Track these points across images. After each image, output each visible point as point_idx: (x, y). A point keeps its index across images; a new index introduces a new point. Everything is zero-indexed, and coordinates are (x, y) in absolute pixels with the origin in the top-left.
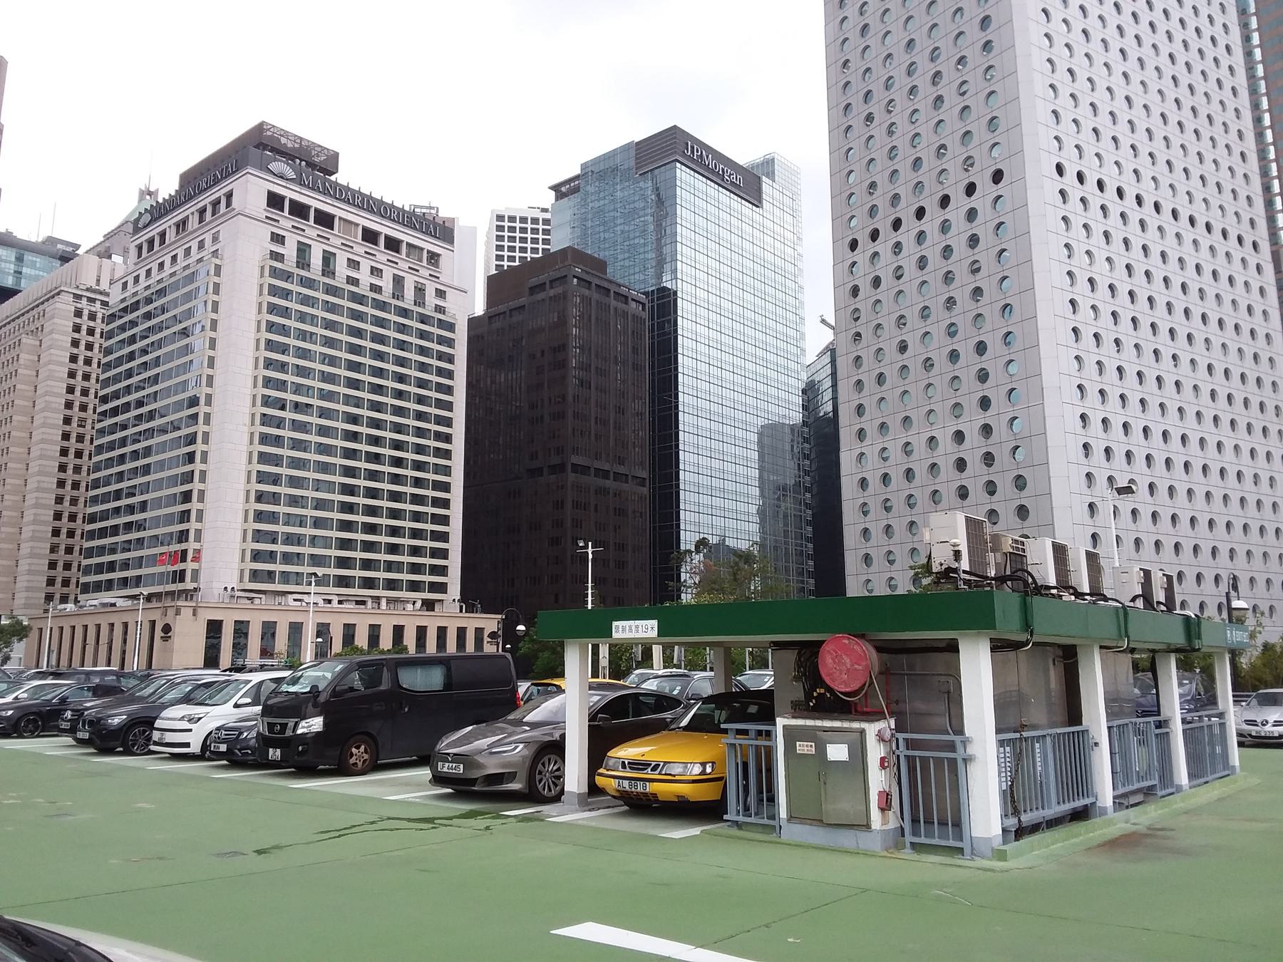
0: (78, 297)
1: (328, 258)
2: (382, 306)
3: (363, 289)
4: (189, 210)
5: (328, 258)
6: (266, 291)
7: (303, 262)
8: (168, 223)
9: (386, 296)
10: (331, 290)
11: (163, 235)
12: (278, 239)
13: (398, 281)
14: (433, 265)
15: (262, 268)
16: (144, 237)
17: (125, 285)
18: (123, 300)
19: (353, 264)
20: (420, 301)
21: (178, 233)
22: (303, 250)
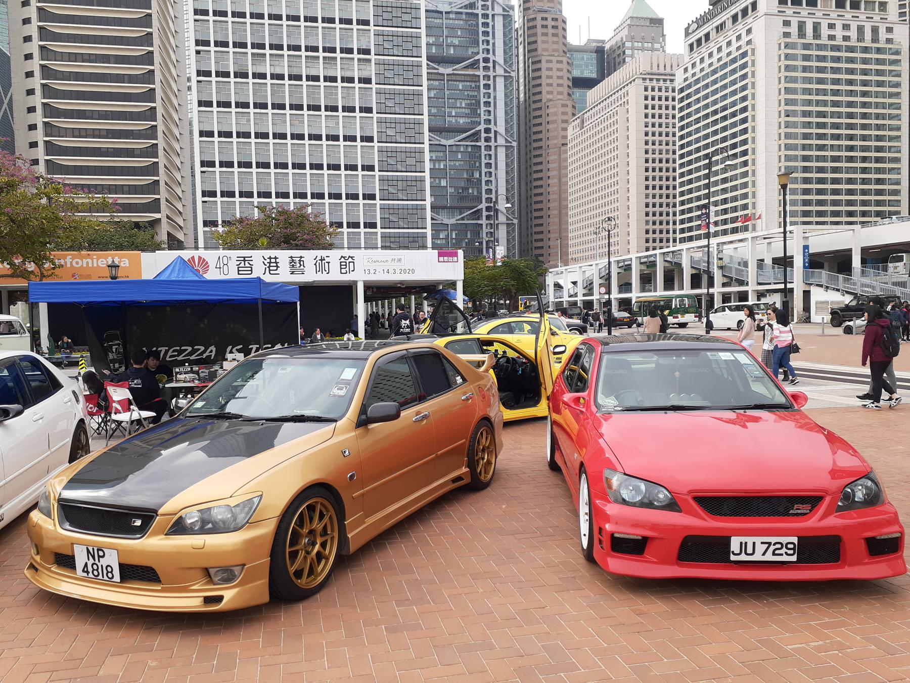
0: (644, 79)
1: (816, 27)
2: (851, 49)
3: (839, 42)
4: (726, 16)
5: (816, 27)
6: (783, 58)
7: (802, 33)
8: (709, 27)
9: (853, 43)
10: (820, 47)
11: (707, 36)
12: (787, 23)
13: (860, 29)
14: (882, 11)
15: (780, 44)
16: (693, 39)
17: (686, 70)
18: (686, 79)
19: (831, 26)
20: (875, 39)
21: (717, 32)
22: (801, 26)
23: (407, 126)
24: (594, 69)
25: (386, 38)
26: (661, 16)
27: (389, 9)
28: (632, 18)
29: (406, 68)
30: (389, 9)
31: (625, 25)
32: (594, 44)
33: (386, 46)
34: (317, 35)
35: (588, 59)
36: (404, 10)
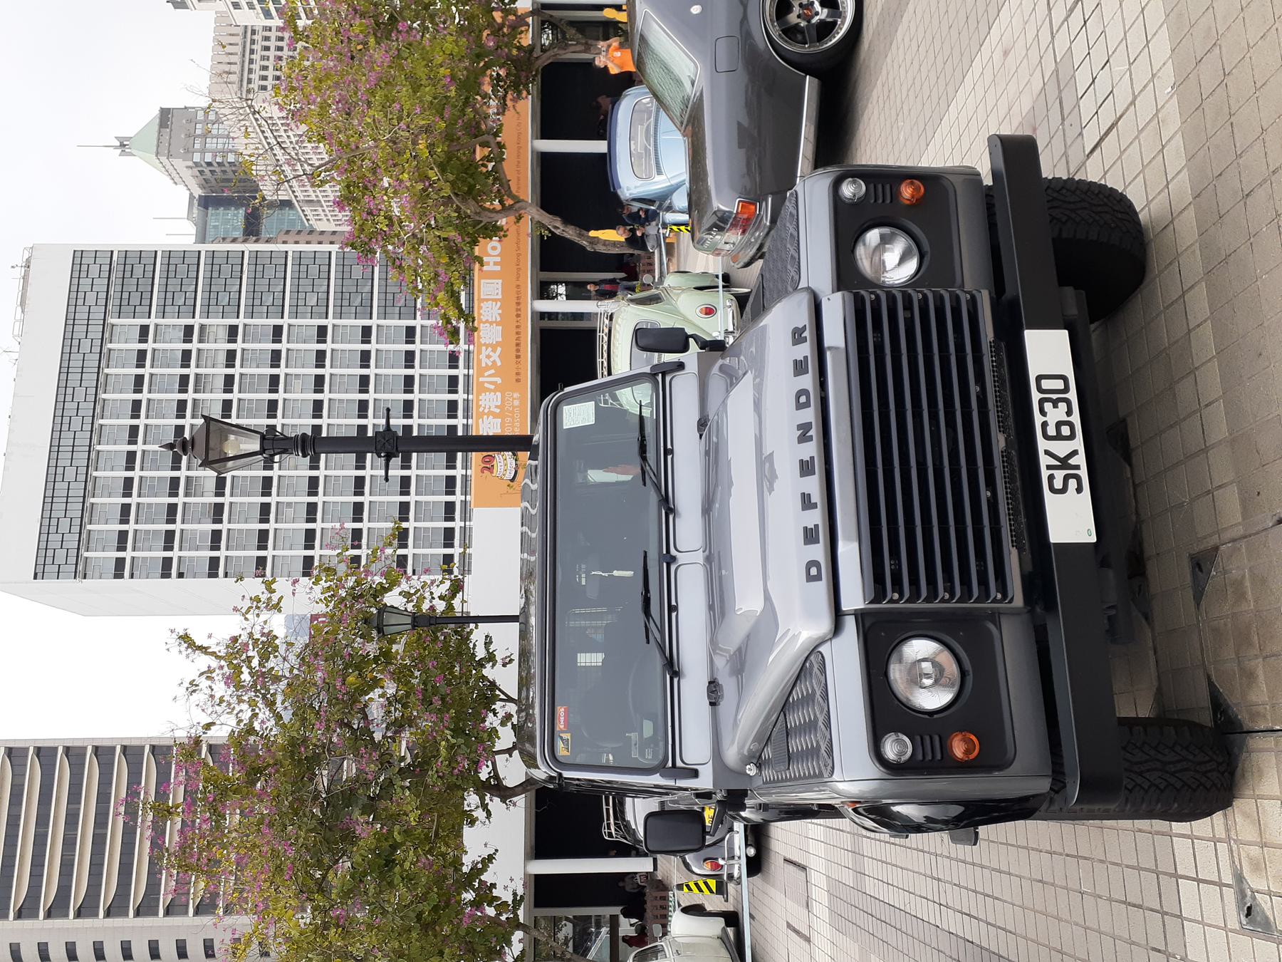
23: (303, 275)
24: (231, 212)
25: (169, 302)
26: (157, 112)
27: (125, 295)
28: (157, 154)
29: (215, 274)
30: (125, 295)
31: (168, 166)
32: (195, 211)
33: (181, 302)
34: (160, 401)
35: (217, 220)
36: (128, 274)
